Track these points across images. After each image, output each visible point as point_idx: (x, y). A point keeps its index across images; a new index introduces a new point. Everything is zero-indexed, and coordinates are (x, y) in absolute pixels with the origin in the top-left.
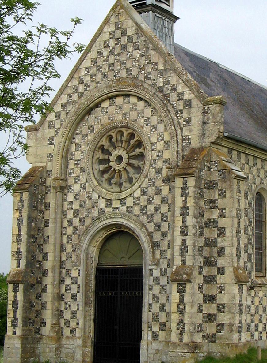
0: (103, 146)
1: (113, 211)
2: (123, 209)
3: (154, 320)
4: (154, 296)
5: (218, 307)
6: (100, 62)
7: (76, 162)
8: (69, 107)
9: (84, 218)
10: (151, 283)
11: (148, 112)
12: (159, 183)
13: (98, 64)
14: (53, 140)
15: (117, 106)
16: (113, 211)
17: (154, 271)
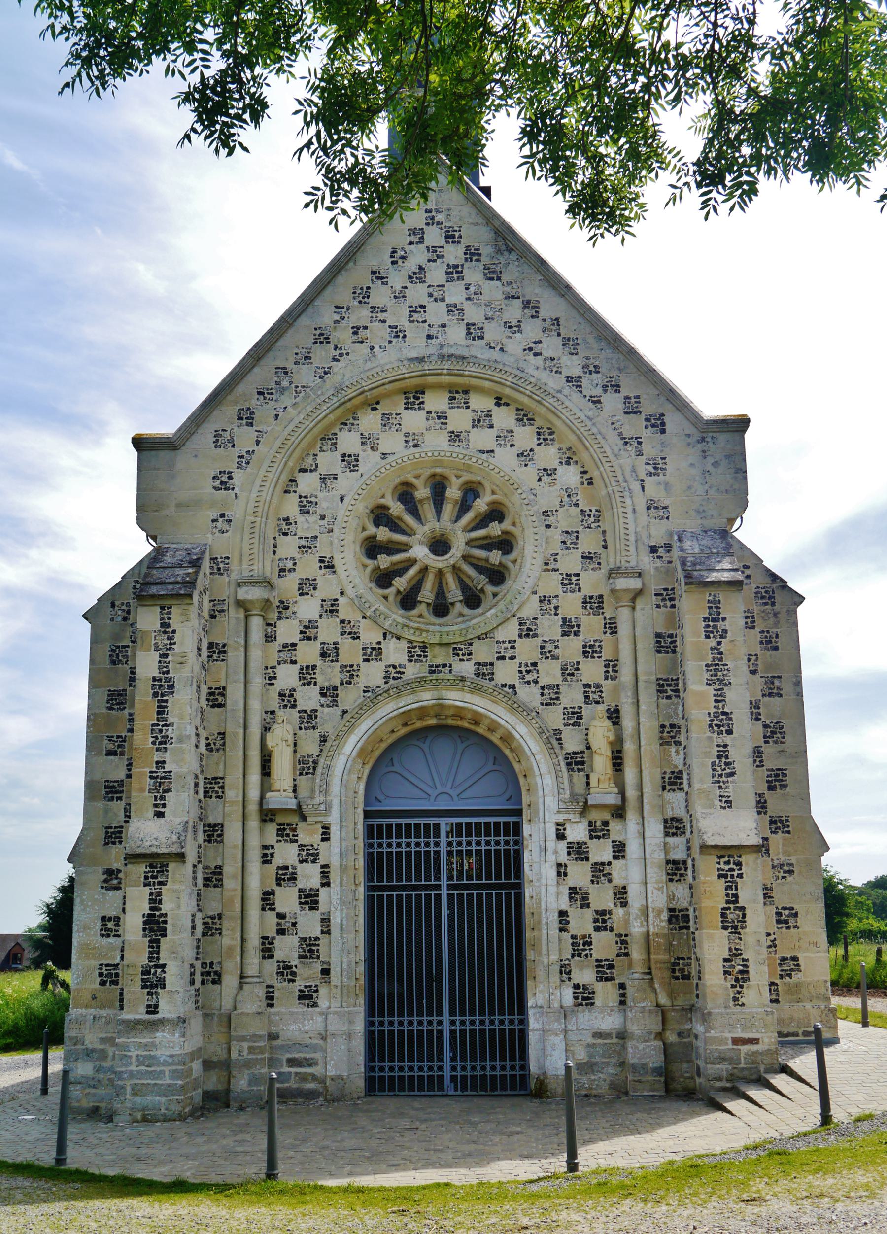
0: (387, 508)
1: (432, 672)
2: (467, 668)
3: (576, 953)
4: (573, 892)
5: (779, 914)
6: (380, 296)
7: (303, 542)
8: (287, 400)
9: (335, 688)
10: (564, 858)
11: (525, 437)
12: (571, 606)
13: (372, 301)
14: (230, 478)
15: (429, 412)
16: (432, 672)
17: (567, 826)
